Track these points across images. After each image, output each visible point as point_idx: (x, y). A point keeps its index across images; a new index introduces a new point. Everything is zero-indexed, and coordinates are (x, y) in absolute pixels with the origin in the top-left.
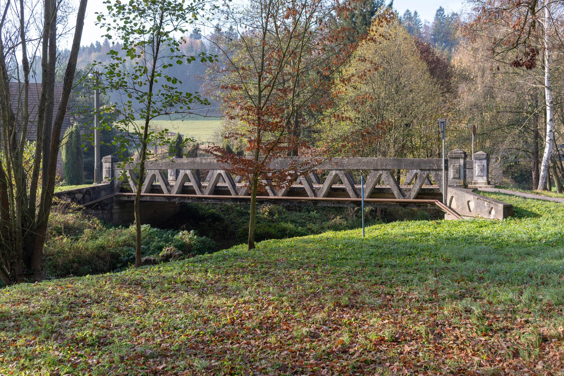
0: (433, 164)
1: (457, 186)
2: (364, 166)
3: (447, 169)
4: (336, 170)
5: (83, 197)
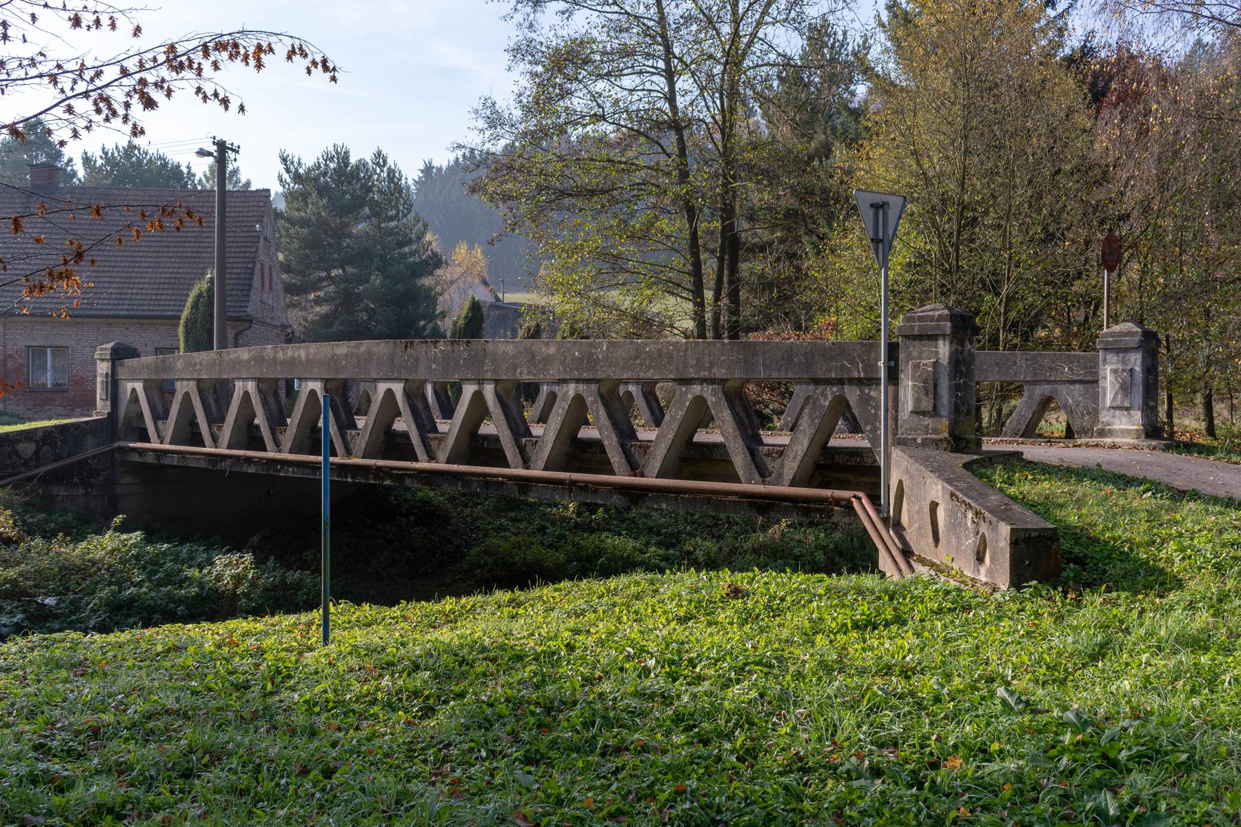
0: (852, 361)
1: (925, 443)
2: (650, 367)
3: (893, 376)
4: (578, 381)
5: (37, 452)
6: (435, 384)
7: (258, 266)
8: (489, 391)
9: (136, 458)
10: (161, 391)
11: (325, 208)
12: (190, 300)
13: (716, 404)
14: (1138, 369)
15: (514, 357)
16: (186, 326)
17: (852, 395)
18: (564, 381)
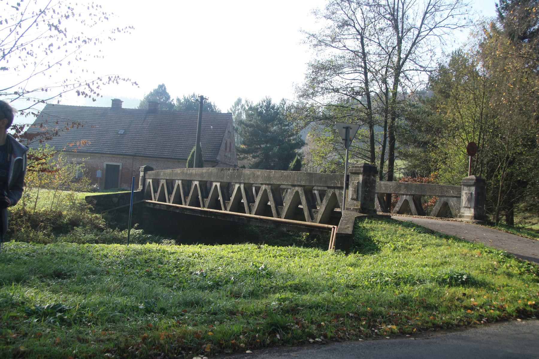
3: (347, 187)
4: (266, 184)
6: (256, 187)
7: (224, 142)
8: (242, 186)
9: (148, 206)
10: (156, 182)
11: (259, 120)
12: (191, 153)
13: (302, 194)
14: (473, 193)
15: (249, 175)
16: (189, 163)
17: (337, 192)
18: (262, 184)
